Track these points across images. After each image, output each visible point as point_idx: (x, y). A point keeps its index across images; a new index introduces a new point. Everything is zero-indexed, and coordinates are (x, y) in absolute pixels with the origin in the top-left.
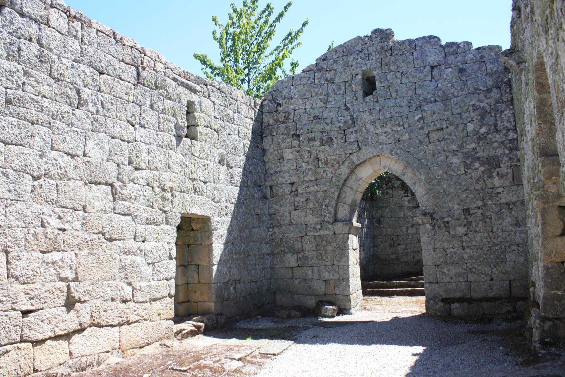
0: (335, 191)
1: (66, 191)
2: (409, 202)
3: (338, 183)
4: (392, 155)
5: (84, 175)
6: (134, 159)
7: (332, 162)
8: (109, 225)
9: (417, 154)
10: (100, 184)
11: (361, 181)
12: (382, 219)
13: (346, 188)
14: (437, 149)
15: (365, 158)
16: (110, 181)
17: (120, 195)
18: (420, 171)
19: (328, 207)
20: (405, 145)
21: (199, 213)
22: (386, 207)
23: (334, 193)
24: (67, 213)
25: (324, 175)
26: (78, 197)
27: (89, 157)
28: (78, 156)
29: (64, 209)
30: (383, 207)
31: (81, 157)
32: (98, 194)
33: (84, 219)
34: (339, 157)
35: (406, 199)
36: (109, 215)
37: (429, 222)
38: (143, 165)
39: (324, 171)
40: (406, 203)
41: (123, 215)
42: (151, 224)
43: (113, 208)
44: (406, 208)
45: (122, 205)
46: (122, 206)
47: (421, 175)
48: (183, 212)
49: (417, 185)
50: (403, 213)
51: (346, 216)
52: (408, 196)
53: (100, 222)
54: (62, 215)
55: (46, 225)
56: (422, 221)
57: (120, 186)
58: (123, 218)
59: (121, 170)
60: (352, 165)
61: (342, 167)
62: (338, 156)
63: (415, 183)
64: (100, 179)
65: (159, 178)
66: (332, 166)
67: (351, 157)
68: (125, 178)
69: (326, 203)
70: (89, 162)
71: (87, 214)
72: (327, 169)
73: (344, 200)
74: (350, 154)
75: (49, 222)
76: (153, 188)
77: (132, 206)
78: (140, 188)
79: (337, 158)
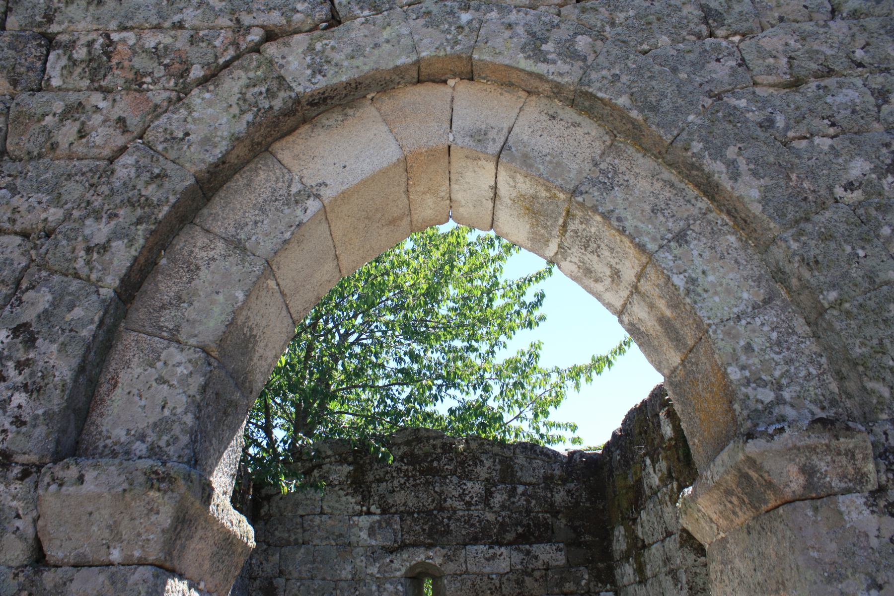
0: (116, 235)
2: (372, 532)
3: (150, 191)
4: (540, 56)
7: (141, 62)
9: (697, 66)
11: (313, 205)
12: (280, 582)
13: (201, 240)
14: (812, 54)
15: (364, 66)
18: (731, 152)
19: (31, 342)
20: (620, 17)
22: (296, 542)
23: (104, 248)
25: (67, 133)
30: (288, 543)
34: (193, 41)
35: (364, 521)
37: (861, 478)
39: (74, 111)
40: (364, 535)
44: (360, 550)
47: (735, 176)
49: (696, 247)
50: (349, 568)
51: (162, 426)
52: (369, 513)
56: (808, 471)
60: (270, 94)
61: (197, 97)
62: (183, 36)
63: (681, 238)
66: (136, 83)
67: (272, 49)
69: (28, 315)
72: (96, 99)
73: (167, 319)
74: (270, 36)
79: (181, 41)
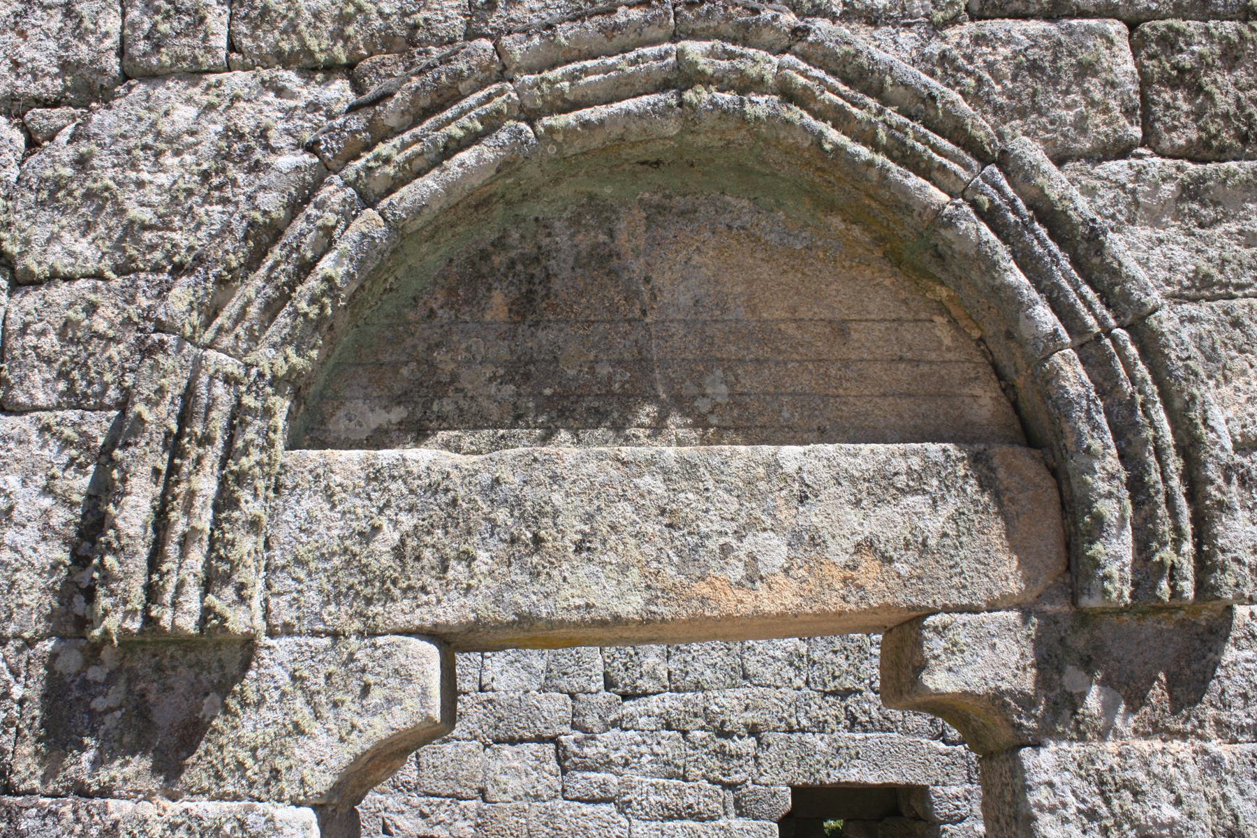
1: (438, 763)
5: (481, 727)
6: (621, 676)
8: (546, 825)
10: (522, 740)
16: (549, 733)
17: (577, 760)
21: (872, 778)
24: (438, 806)
26: (465, 773)
27: (493, 690)
28: (465, 694)
29: (431, 799)
31: (473, 694)
32: (516, 764)
33: (479, 815)
36: (548, 804)
38: (646, 684)
41: (588, 802)
42: (681, 818)
43: (559, 788)
45: (581, 781)
46: (584, 782)
48: (800, 781)
53: (523, 821)
54: (426, 810)
55: (393, 830)
57: (575, 741)
58: (587, 809)
59: (579, 706)
64: (521, 732)
65: (705, 709)
68: (592, 720)
70: (490, 701)
71: (486, 807)
75: (399, 823)
76: (685, 733)
77: (615, 780)
78: (639, 739)
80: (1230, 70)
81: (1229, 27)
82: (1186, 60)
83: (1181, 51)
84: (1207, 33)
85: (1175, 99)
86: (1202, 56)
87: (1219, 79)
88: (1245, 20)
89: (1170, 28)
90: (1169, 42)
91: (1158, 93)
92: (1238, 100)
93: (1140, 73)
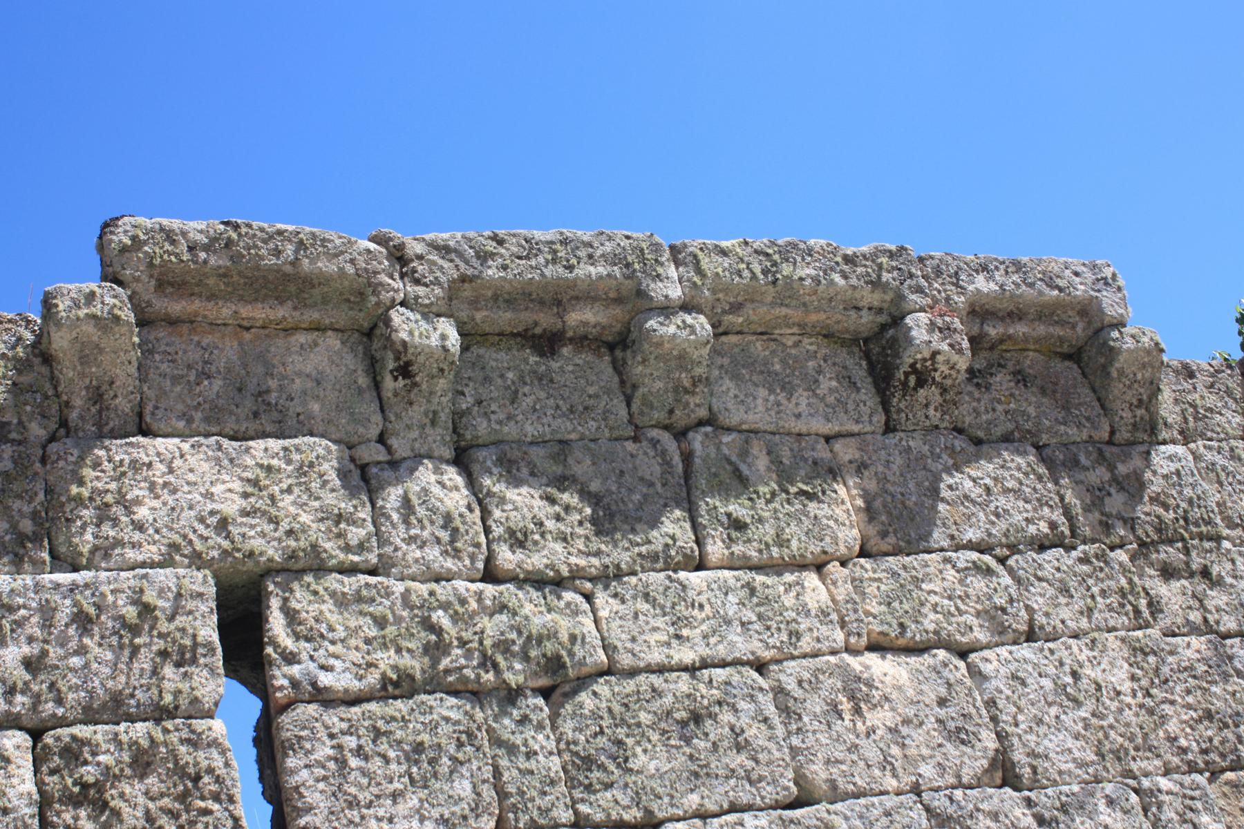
80: (142, 777)
81: (140, 730)
82: (89, 773)
83: (86, 763)
84: (116, 738)
85: (76, 818)
86: (108, 768)
87: (128, 790)
88: (158, 721)
89: (74, 738)
90: (73, 753)
91: (58, 814)
92: (147, 812)
93: (40, 791)
